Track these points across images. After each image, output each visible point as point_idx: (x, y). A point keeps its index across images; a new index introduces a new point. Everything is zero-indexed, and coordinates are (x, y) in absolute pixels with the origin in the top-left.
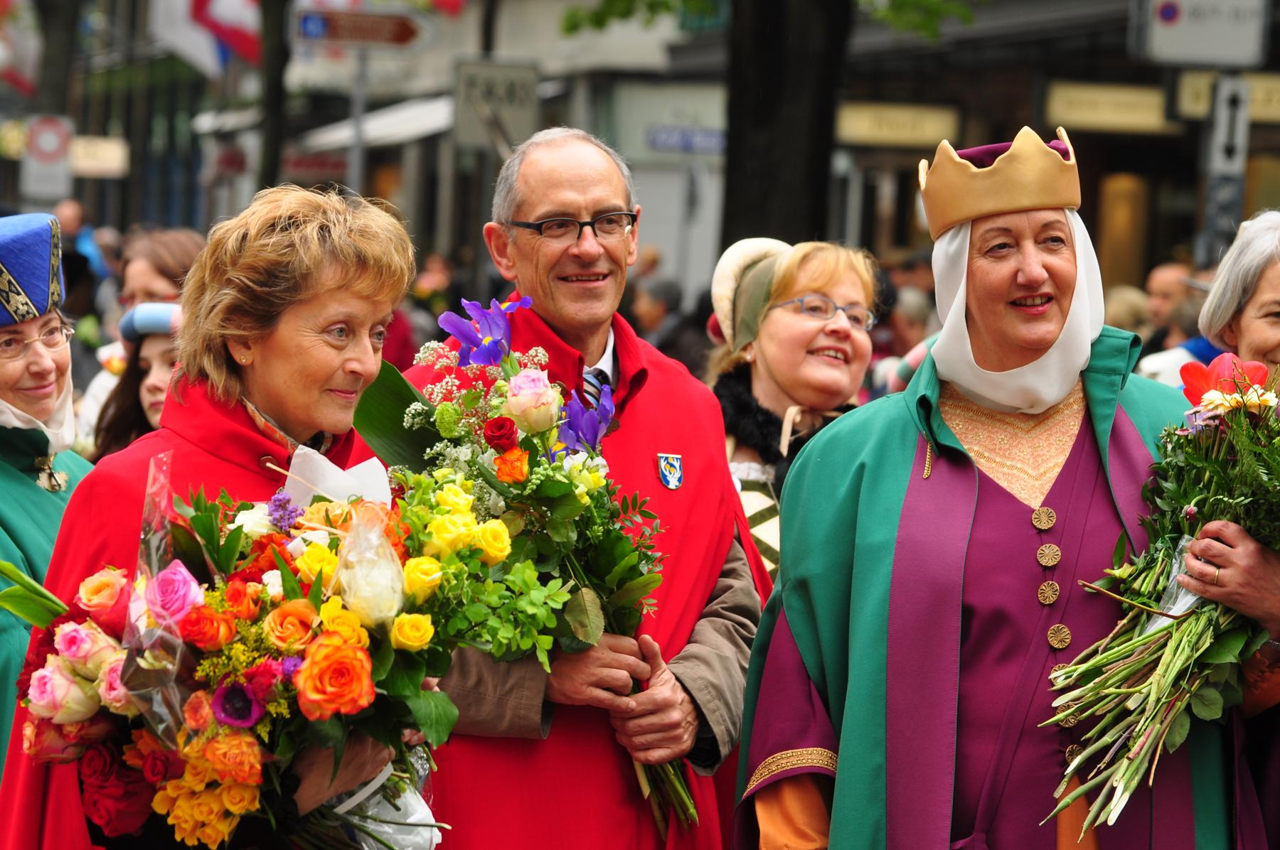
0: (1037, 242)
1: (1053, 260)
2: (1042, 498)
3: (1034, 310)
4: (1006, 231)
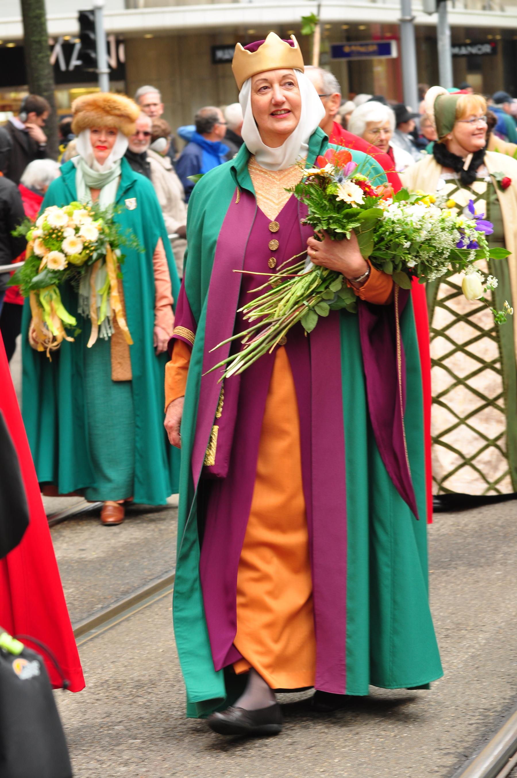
0: (281, 85)
1: (289, 94)
2: (277, 214)
3: (281, 116)
4: (266, 80)
